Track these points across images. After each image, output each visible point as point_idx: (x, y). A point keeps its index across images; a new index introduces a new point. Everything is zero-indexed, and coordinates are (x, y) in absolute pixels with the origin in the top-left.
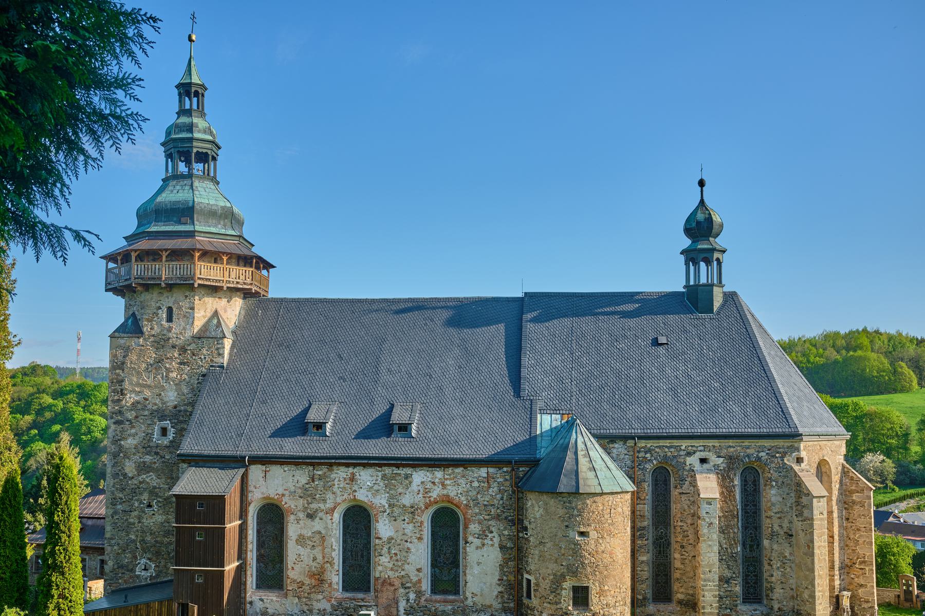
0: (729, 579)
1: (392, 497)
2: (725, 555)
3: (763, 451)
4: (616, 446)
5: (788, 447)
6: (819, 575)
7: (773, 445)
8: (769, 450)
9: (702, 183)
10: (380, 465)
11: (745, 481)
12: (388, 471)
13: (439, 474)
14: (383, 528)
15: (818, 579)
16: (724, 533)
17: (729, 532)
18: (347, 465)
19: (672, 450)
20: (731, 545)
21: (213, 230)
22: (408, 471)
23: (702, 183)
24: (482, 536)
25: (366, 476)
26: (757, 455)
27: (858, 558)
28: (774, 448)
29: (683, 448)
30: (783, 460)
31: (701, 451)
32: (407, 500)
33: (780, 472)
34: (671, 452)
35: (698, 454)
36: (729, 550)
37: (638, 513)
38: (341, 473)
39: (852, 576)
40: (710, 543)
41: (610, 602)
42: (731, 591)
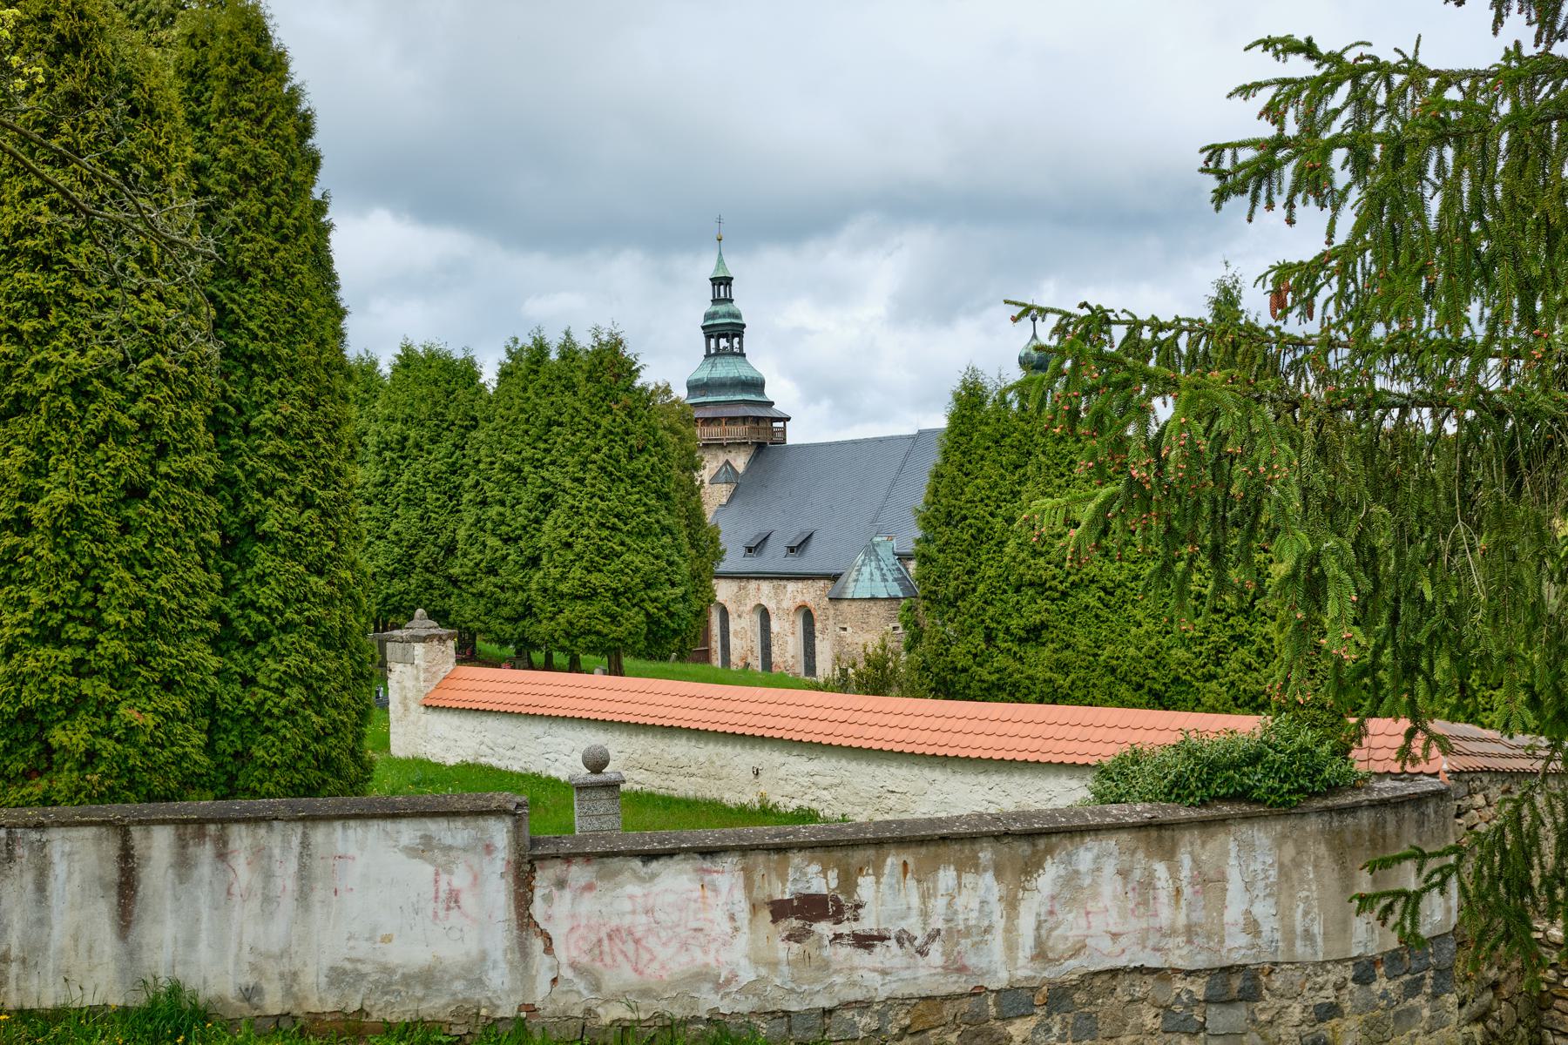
1: (779, 602)
10: (772, 578)
12: (775, 582)
13: (800, 585)
14: (775, 626)
18: (756, 578)
21: (722, 398)
22: (783, 583)
24: (822, 632)
25: (766, 586)
32: (785, 605)
38: (753, 584)
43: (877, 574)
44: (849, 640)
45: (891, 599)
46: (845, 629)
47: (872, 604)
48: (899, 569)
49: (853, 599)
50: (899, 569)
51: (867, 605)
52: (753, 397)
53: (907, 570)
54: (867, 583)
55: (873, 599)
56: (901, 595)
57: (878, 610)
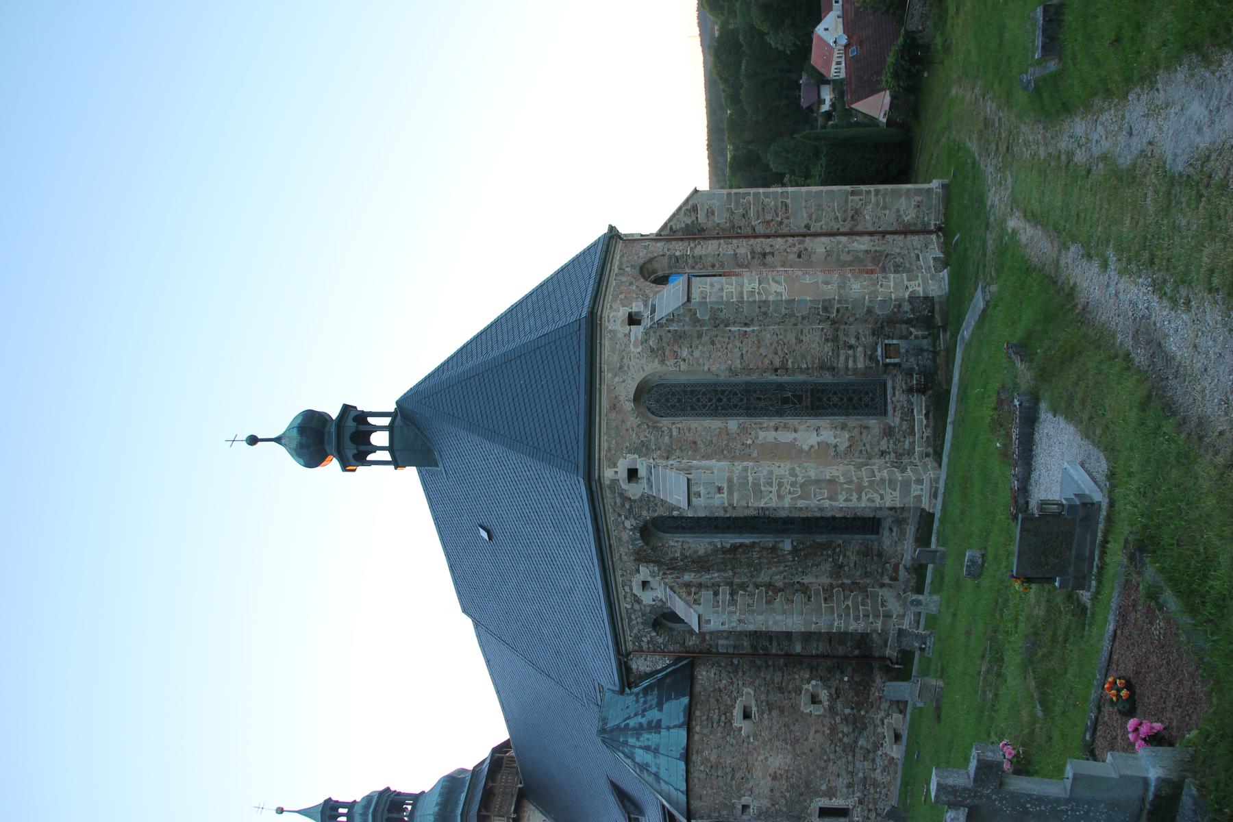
0: (835, 564)
2: (796, 569)
3: (623, 523)
4: (634, 667)
5: (613, 492)
6: (830, 498)
7: (611, 511)
8: (620, 515)
9: (253, 440)
11: (676, 528)
15: (836, 500)
16: (761, 569)
17: (760, 564)
19: (633, 617)
20: (779, 562)
23: (253, 440)
26: (631, 530)
27: (818, 314)
28: (617, 510)
29: (629, 606)
30: (635, 501)
31: (631, 589)
33: (656, 505)
34: (636, 618)
35: (635, 592)
36: (790, 563)
37: (731, 651)
39: (851, 319)
40: (771, 623)
41: (845, 782)
42: (855, 564)
43: (650, 738)
44: (766, 803)
45: (688, 725)
46: (745, 807)
47: (695, 758)
48: (646, 691)
49: (688, 793)
50: (646, 691)
51: (699, 769)
52: (463, 796)
53: (648, 675)
54: (662, 761)
55: (687, 757)
56: (685, 700)
57: (707, 753)
